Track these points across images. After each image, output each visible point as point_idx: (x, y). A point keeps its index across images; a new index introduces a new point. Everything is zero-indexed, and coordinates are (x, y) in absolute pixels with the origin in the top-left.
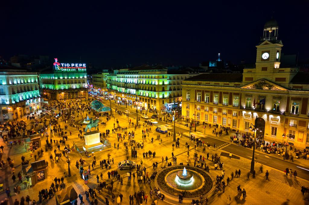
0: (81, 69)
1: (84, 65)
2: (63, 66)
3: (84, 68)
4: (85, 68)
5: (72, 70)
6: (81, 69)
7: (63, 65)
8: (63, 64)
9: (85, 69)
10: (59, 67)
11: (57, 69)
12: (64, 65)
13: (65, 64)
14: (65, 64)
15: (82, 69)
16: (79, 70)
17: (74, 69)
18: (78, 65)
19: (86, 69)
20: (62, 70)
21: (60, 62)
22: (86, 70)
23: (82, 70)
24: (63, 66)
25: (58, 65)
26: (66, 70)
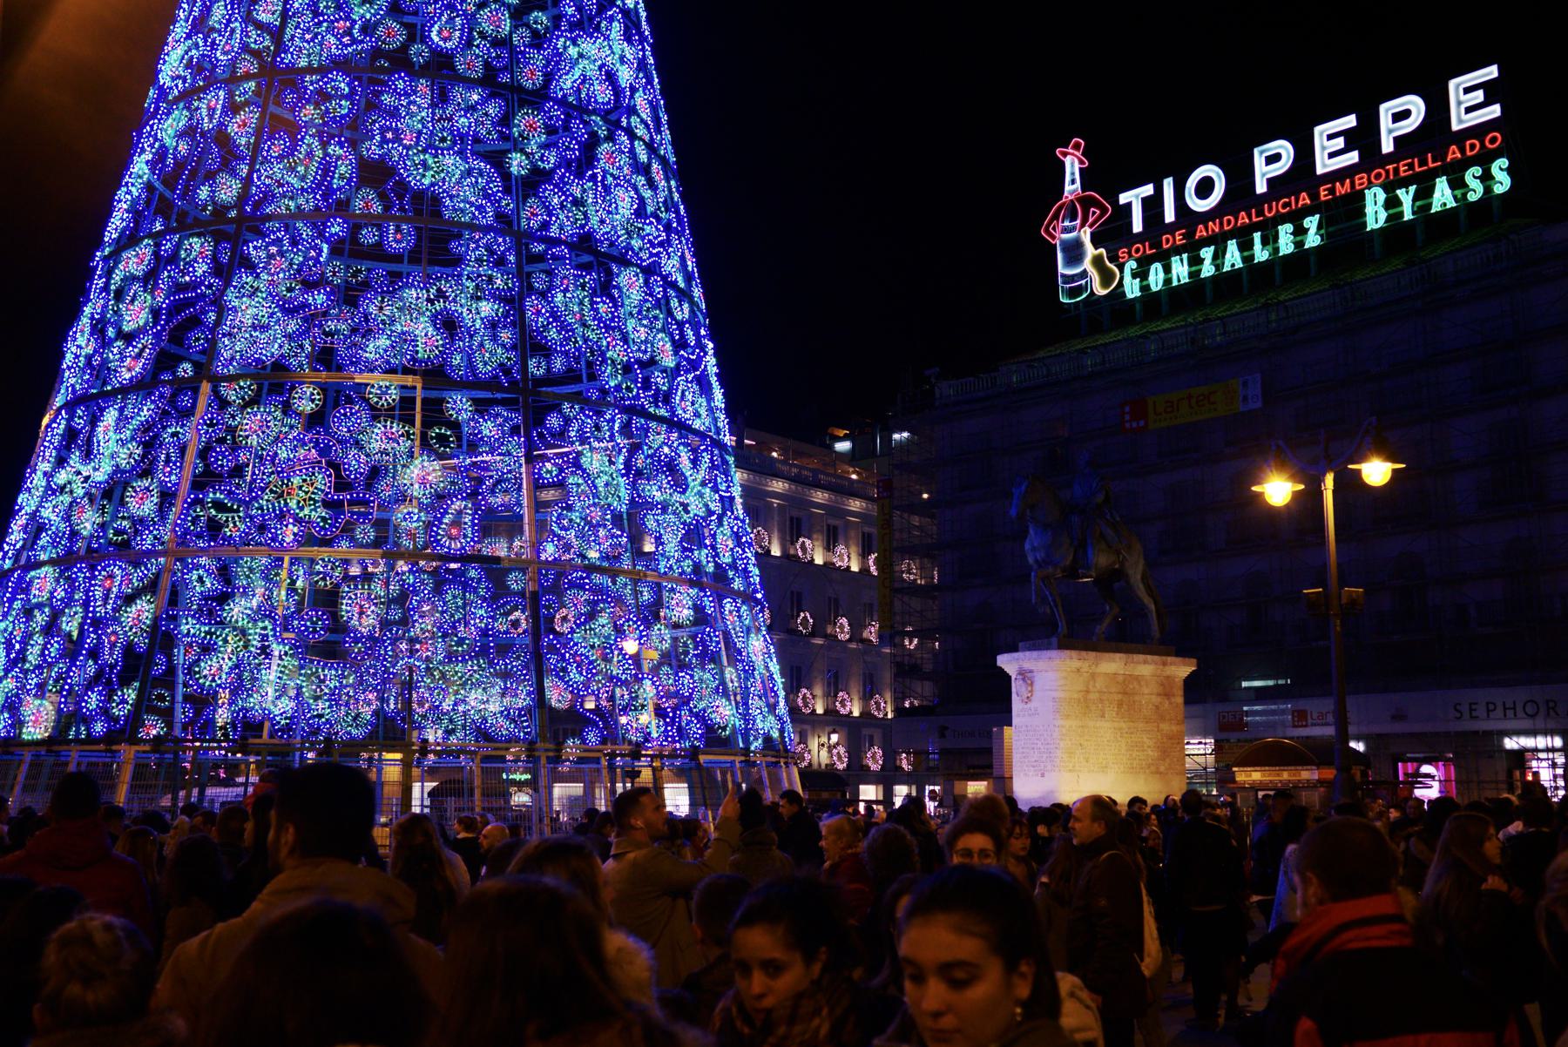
0: (1406, 196)
1: (1468, 101)
2: (1137, 227)
3: (1473, 147)
4: (1495, 139)
5: (1261, 254)
6: (1406, 196)
7: (1145, 200)
8: (1133, 198)
9: (1485, 159)
10: (1098, 261)
11: (1074, 292)
12: (1153, 206)
13: (1168, 185)
14: (1168, 185)
15: (1425, 193)
16: (1375, 215)
17: (1296, 218)
18: (1363, 138)
19: (1499, 167)
20: (1132, 289)
21: (1104, 179)
22: (1503, 182)
23: (1443, 196)
24: (1137, 227)
25: (1086, 235)
26: (1180, 270)
